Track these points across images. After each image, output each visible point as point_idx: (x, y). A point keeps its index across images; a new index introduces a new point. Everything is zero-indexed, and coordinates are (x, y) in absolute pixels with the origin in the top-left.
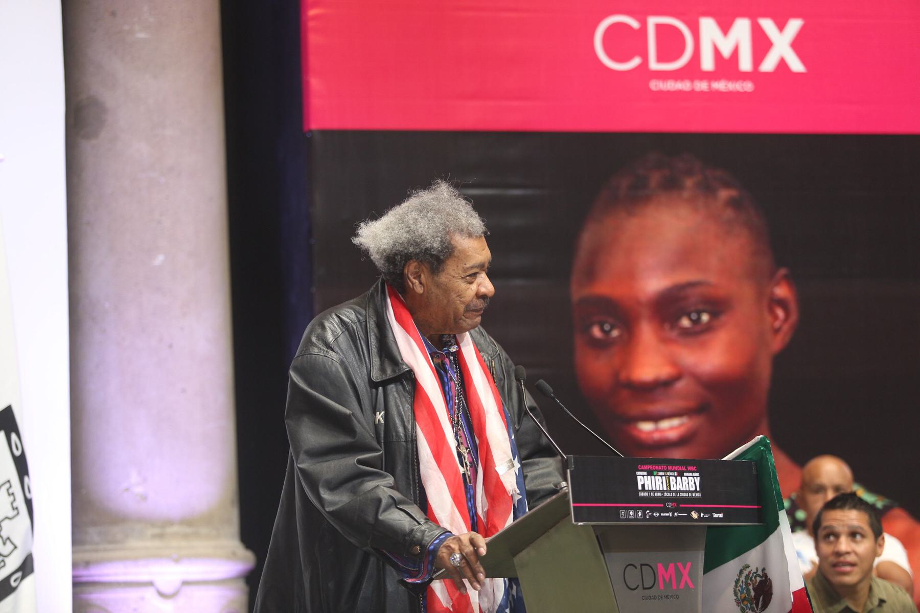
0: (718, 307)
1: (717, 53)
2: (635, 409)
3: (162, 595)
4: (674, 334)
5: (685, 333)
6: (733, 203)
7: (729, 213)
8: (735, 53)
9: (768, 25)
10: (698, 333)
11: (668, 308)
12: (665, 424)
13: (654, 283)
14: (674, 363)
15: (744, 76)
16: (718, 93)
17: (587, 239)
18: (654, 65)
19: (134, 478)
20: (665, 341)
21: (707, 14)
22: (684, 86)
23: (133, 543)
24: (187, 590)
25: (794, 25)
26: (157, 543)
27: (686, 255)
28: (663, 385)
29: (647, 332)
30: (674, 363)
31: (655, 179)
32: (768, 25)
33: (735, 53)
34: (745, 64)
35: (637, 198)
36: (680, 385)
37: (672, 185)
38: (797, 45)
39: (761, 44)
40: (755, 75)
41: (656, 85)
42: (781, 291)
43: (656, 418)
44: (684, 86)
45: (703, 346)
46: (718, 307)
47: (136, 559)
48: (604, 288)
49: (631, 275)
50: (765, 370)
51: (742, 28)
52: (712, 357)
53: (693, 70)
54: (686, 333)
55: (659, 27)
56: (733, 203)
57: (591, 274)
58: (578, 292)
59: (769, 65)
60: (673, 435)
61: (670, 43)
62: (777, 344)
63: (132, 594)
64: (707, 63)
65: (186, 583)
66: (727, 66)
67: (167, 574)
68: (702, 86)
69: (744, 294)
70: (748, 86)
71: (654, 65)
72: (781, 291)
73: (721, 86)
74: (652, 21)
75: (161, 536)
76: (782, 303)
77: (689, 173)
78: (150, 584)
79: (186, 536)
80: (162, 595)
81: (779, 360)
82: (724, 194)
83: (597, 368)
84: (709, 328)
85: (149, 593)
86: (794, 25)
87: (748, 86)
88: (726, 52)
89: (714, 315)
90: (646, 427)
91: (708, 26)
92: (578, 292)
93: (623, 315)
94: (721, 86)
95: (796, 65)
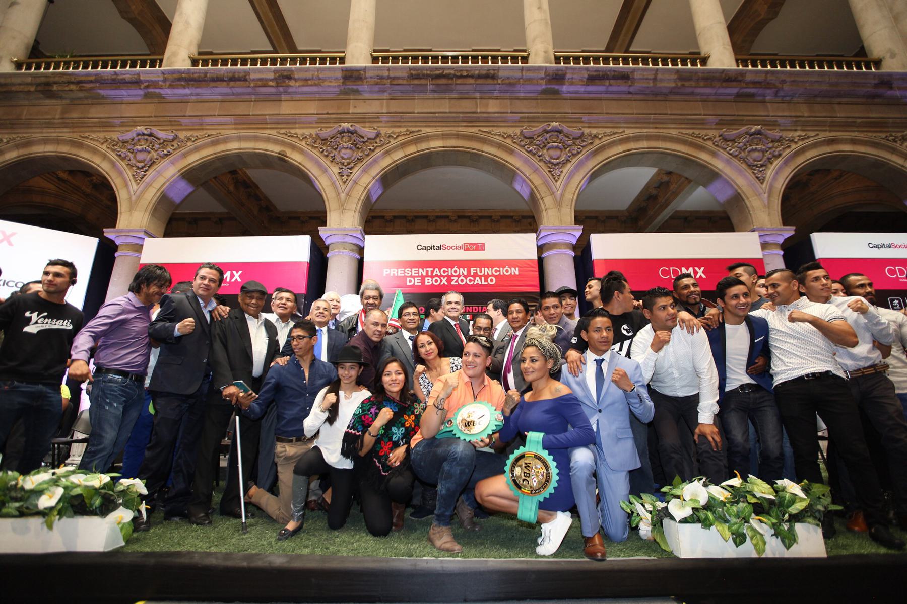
25: (240, 272)
86: (240, 272)
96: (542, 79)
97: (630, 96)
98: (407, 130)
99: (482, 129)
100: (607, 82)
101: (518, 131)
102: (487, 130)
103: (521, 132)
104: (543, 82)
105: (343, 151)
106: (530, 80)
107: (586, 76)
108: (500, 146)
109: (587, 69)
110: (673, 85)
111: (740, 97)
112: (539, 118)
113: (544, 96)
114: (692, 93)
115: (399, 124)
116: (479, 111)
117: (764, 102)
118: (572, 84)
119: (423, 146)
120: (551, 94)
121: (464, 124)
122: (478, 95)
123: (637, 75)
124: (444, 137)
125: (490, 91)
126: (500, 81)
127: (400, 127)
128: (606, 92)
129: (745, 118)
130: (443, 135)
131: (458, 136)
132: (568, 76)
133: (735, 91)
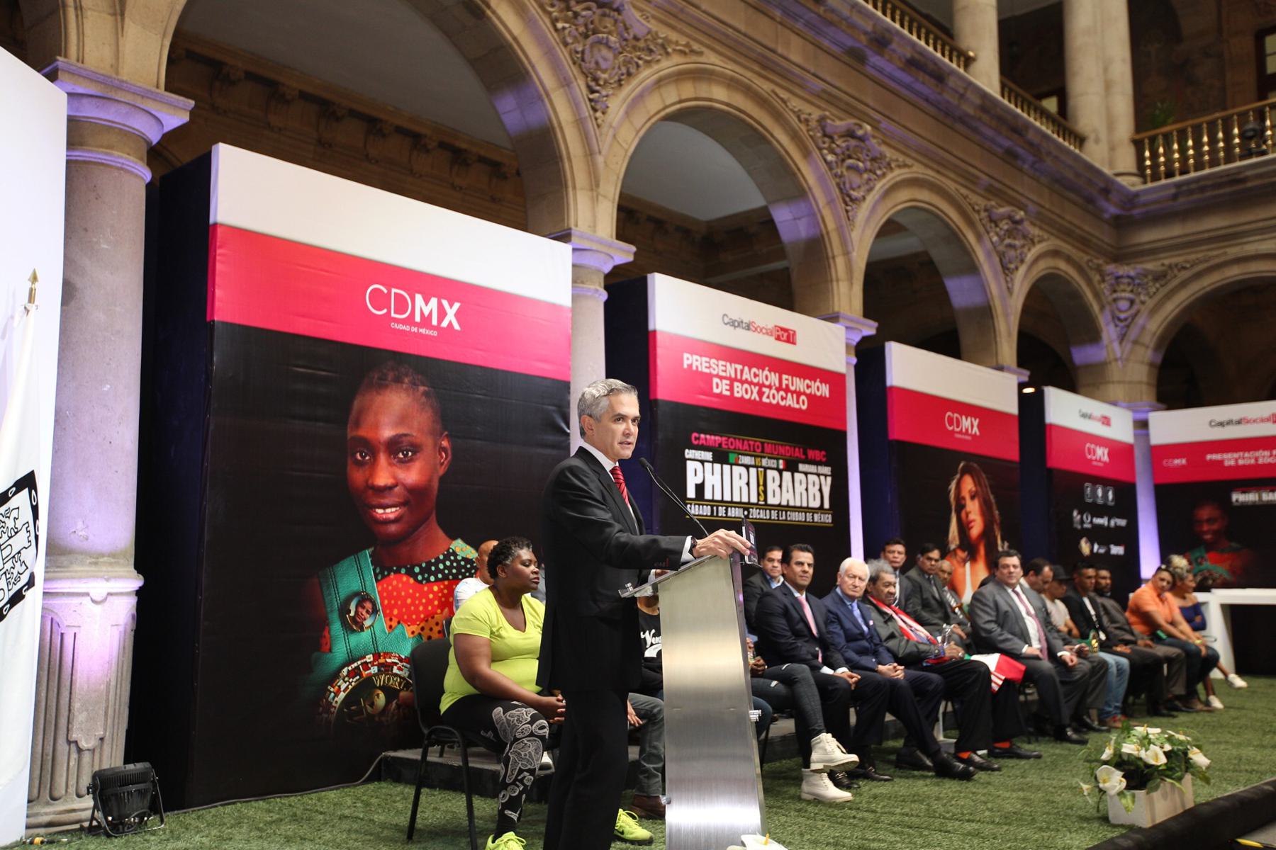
0: (416, 448)
1: (422, 313)
2: (375, 501)
3: (93, 601)
4: (395, 461)
5: (401, 461)
6: (426, 394)
7: (424, 399)
8: (431, 313)
9: (445, 303)
10: (406, 462)
11: (394, 447)
12: (388, 510)
13: (387, 433)
14: (394, 477)
15: (433, 328)
16: (422, 334)
17: (356, 404)
18: (393, 315)
19: (80, 525)
20: (390, 464)
21: (419, 292)
22: (406, 328)
23: (75, 568)
24: (110, 598)
26: (93, 568)
27: (403, 419)
28: (390, 488)
29: (383, 459)
30: (394, 477)
31: (390, 376)
32: (445, 303)
33: (431, 313)
34: (435, 322)
35: (381, 386)
36: (396, 489)
37: (398, 380)
38: (457, 315)
39: (442, 314)
40: (438, 328)
41: (394, 325)
42: (445, 443)
43: (384, 507)
44: (406, 328)
45: (408, 469)
46: (416, 448)
47: (80, 578)
48: (362, 432)
49: (376, 427)
50: (435, 485)
51: (434, 301)
52: (412, 476)
53: (410, 320)
54: (401, 461)
55: (396, 294)
56: (426, 394)
57: (357, 424)
58: (351, 434)
59: (445, 324)
60: (392, 516)
61: (401, 305)
62: (441, 471)
63: (75, 601)
64: (418, 319)
65: (110, 594)
66: (426, 321)
67: (98, 588)
68: (415, 329)
69: (428, 442)
70: (435, 333)
71: (393, 315)
72: (445, 443)
73: (422, 331)
74: (394, 291)
75: (96, 564)
76: (444, 450)
77: (407, 375)
78: (88, 594)
79: (111, 564)
80: (93, 601)
81: (442, 480)
82: (422, 388)
83: (358, 476)
84: (411, 460)
85: (86, 600)
86: (457, 305)
87: (435, 333)
88: (426, 313)
89: (414, 453)
90: (380, 511)
91: (419, 298)
92: (351, 434)
93: (371, 448)
94: (422, 331)
95: (457, 327)
96: (866, 33)
97: (924, 104)
98: (687, 45)
99: (778, 90)
100: (921, 76)
101: (816, 114)
102: (784, 95)
103: (822, 120)
104: (863, 38)
105: (605, 52)
106: (853, 26)
107: (909, 55)
108: (795, 136)
109: (914, 45)
110: (971, 111)
111: (1010, 156)
112: (840, 99)
113: (846, 58)
114: (975, 130)
115: (672, 21)
116: (780, 50)
117: (1020, 170)
118: (890, 61)
119: (767, 121)
120: (856, 57)
121: (757, 68)
122: (778, 14)
123: (952, 82)
124: (733, 83)
125: (795, 17)
126: (821, 10)
127: (673, 28)
128: (908, 87)
129: (1010, 192)
130: (732, 79)
131: (748, 91)
132: (894, 46)
133: (1007, 143)
